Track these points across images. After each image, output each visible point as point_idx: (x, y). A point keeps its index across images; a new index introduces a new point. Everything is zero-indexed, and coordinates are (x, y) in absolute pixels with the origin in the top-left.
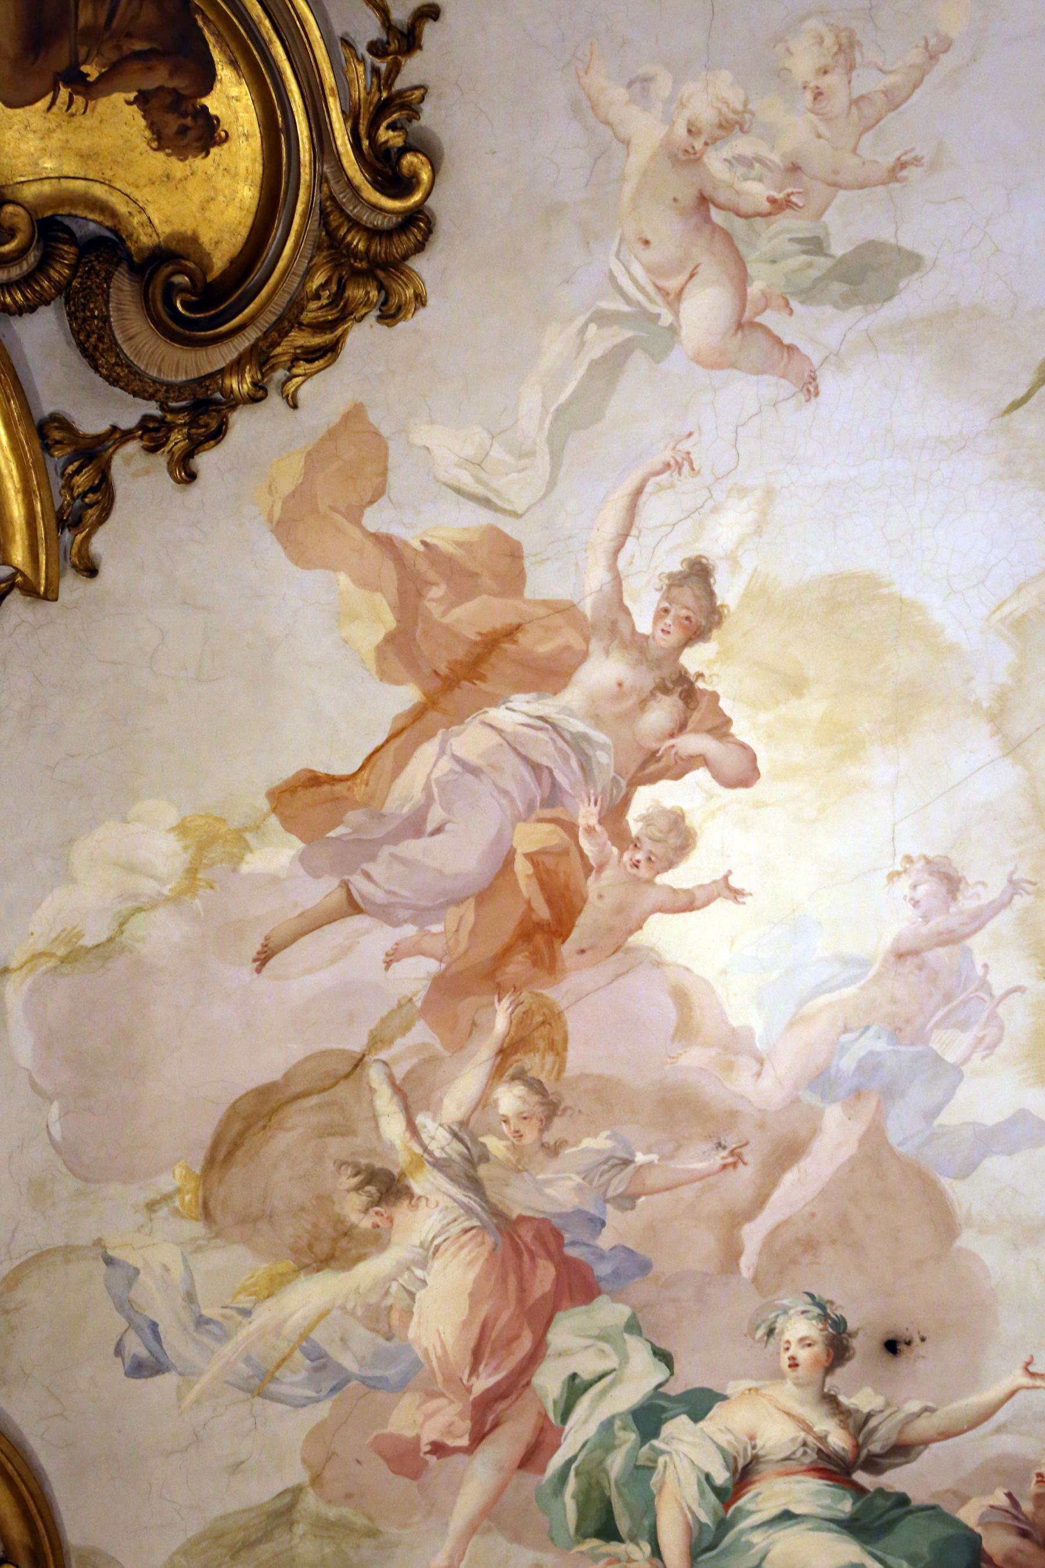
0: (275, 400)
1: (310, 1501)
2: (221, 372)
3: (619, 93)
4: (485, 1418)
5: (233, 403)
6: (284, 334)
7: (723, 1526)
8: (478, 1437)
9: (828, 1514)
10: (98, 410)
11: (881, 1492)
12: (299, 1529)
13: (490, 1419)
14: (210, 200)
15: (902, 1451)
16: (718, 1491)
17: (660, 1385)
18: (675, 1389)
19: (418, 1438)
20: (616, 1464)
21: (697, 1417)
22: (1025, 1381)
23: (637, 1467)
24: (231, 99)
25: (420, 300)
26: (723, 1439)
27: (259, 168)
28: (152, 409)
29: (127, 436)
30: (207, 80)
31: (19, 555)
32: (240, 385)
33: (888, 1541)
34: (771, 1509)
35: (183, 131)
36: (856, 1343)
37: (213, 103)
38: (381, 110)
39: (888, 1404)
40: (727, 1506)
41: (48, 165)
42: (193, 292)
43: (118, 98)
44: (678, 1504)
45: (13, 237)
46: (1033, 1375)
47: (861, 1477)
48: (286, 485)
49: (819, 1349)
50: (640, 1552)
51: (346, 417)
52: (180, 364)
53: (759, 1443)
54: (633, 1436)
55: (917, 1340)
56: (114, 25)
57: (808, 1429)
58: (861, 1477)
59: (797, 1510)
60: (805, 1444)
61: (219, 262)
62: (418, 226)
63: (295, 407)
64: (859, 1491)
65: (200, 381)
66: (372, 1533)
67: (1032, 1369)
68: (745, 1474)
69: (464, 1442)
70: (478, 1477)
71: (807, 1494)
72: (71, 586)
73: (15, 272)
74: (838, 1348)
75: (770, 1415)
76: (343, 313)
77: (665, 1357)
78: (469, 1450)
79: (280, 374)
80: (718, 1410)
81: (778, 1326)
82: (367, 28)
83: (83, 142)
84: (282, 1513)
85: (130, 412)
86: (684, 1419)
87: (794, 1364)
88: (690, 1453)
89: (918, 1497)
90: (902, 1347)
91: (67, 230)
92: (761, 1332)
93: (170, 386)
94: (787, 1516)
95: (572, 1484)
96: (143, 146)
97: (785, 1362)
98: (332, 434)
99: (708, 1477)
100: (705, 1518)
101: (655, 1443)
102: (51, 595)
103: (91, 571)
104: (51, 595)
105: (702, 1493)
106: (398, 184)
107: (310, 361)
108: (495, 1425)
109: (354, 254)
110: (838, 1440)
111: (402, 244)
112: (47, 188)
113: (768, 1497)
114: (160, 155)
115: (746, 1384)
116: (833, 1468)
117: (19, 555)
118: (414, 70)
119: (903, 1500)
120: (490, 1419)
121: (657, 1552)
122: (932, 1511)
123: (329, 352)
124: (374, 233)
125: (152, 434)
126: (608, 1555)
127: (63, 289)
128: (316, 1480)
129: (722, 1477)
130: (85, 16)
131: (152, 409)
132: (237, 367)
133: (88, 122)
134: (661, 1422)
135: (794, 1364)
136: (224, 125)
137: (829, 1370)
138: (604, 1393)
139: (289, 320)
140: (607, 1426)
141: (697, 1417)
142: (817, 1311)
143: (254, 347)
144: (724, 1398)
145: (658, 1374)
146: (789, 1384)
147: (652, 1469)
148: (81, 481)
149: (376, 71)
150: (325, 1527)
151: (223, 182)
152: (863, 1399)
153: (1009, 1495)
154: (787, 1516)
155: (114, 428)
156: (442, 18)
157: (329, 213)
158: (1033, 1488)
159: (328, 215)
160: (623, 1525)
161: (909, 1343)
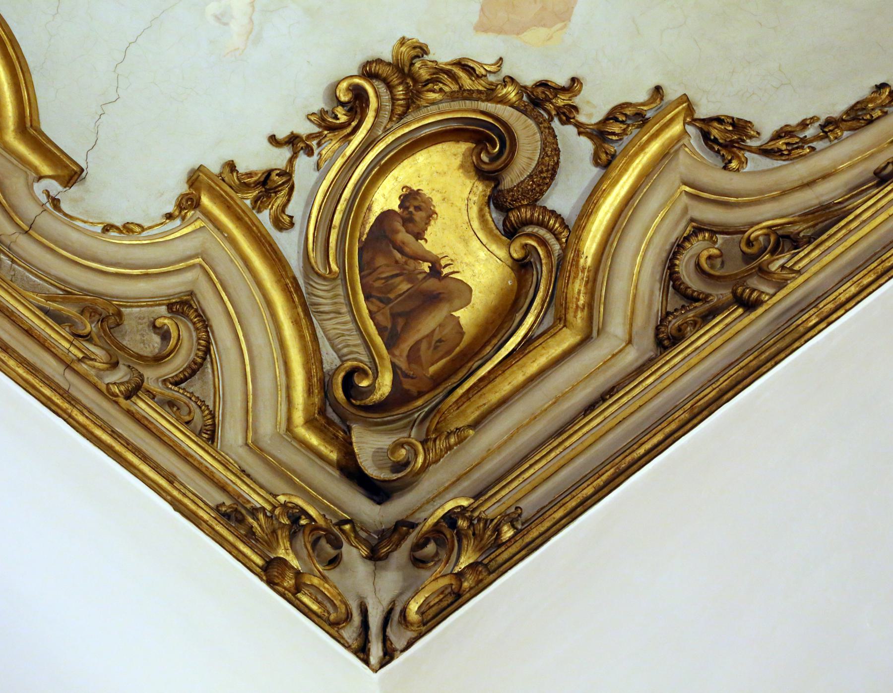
0: (506, 71)
2: (512, 106)
3: (234, 27)
5: (522, 89)
6: (471, 92)
10: (577, 148)
14: (440, 174)
24: (386, 197)
25: (403, 41)
27: (406, 162)
28: (556, 124)
29: (578, 125)
30: (386, 215)
31: (676, 128)
32: (511, 92)
35: (418, 208)
37: (395, 205)
38: (333, 128)
41: (482, 254)
42: (488, 147)
43: (428, 247)
45: (526, 245)
48: (543, 32)
51: (486, 31)
52: (525, 129)
56: (398, 272)
61: (463, 147)
62: (370, 71)
63: (501, 59)
65: (524, 112)
72: (672, 93)
73: (542, 232)
76: (439, 72)
79: (492, 78)
82: (304, 165)
83: (460, 247)
85: (566, 133)
91: (504, 224)
93: (538, 124)
96: (439, 220)
98: (500, 31)
102: (685, 98)
103: (658, 89)
104: (685, 98)
106: (359, 95)
107: (473, 69)
109: (407, 88)
111: (384, 71)
112: (494, 248)
114: (437, 210)
117: (676, 128)
118: (305, 128)
123: (461, 64)
124: (390, 87)
125: (567, 115)
127: (533, 204)
130: (405, 286)
131: (556, 124)
132: (503, 101)
133: (448, 251)
136: (400, 192)
139: (463, 94)
143: (489, 99)
148: (617, 128)
149: (319, 144)
151: (426, 174)
155: (580, 133)
156: (272, 134)
157: (399, 117)
159: (399, 115)
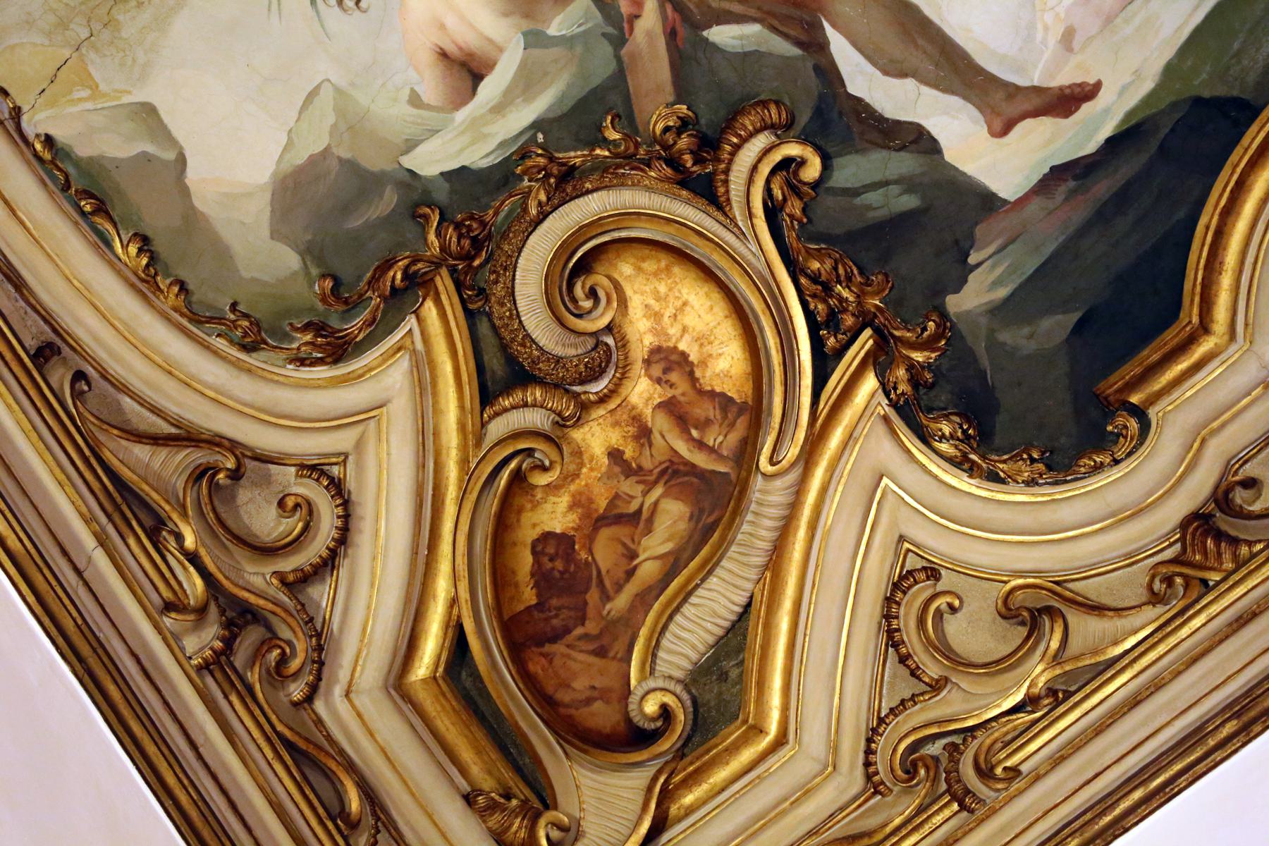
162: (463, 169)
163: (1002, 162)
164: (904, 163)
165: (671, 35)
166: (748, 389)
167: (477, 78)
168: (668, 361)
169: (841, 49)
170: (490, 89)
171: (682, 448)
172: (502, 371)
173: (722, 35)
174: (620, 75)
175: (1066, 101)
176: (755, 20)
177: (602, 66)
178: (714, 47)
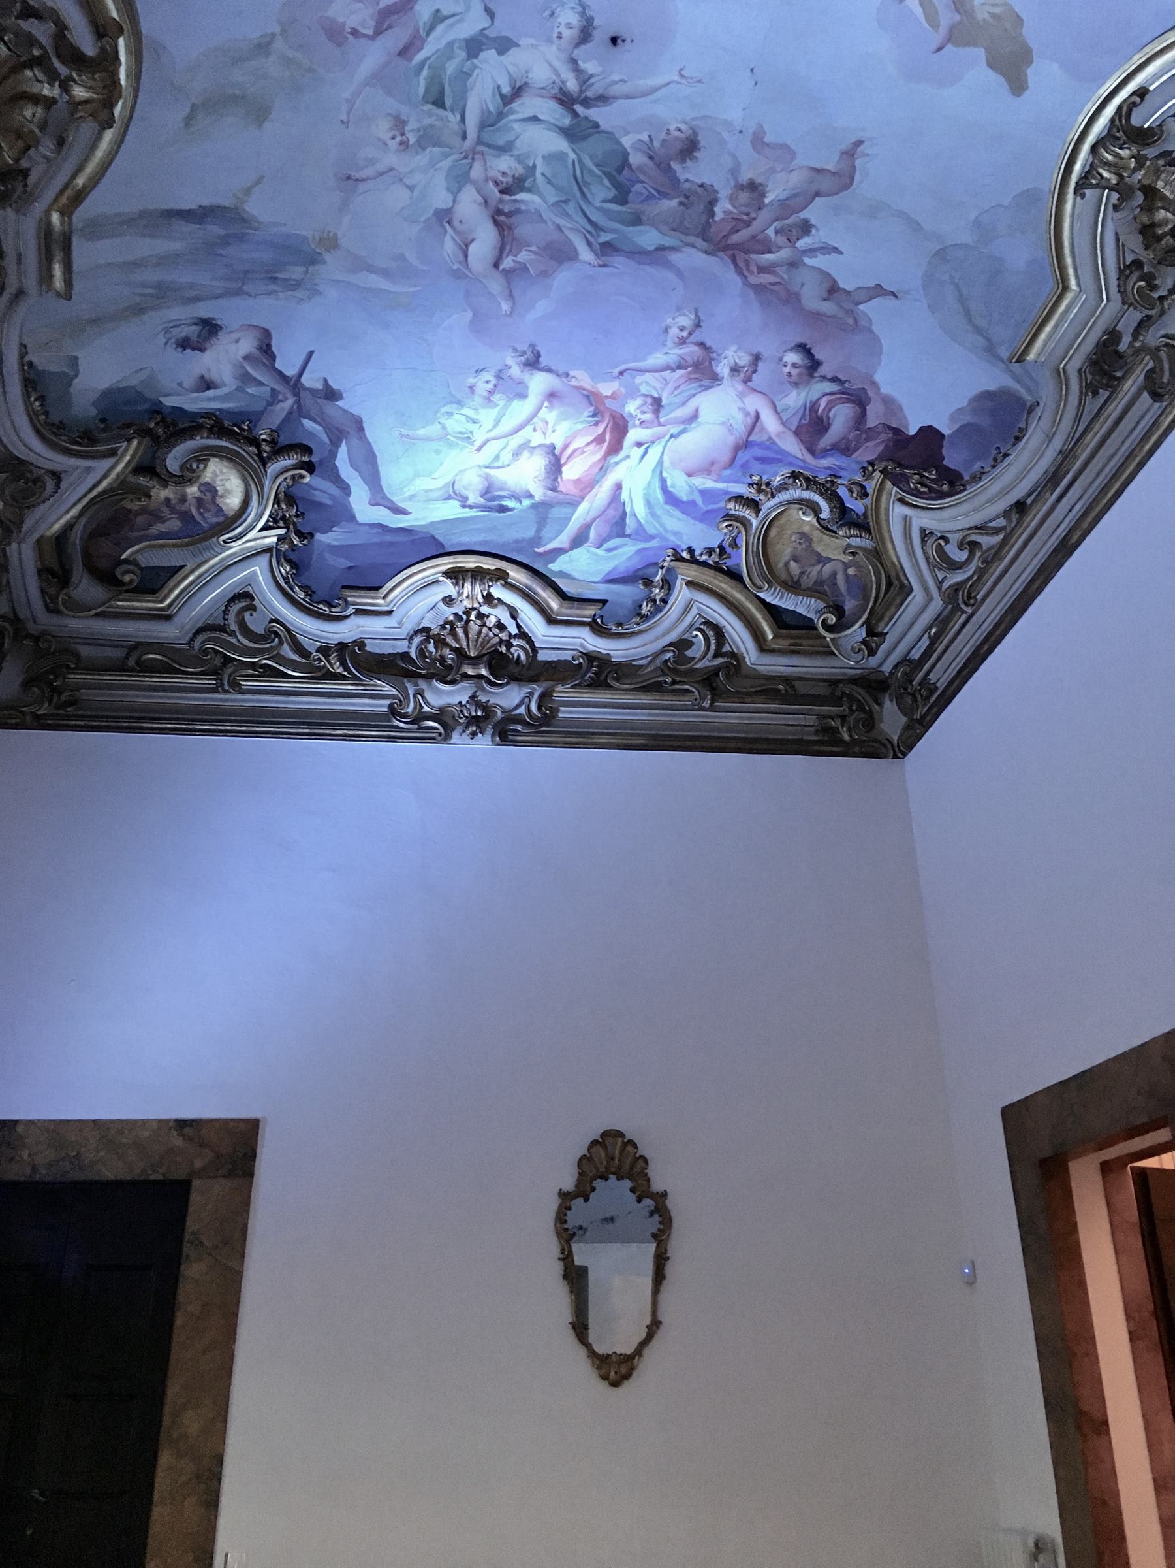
1: (279, 45)
4: (384, 21)
7: (501, 115)
8: (378, 32)
9: (558, 123)
11: (586, 118)
12: (271, 59)
13: (386, 24)
15: (603, 99)
16: (502, 96)
17: (484, 29)
18: (492, 33)
19: (344, 23)
20: (451, 67)
21: (502, 51)
22: (677, 78)
23: (462, 72)
26: (511, 69)
33: (585, 144)
34: (529, 113)
36: (596, 33)
39: (603, 72)
40: (505, 105)
44: (480, 97)
46: (682, 76)
47: (578, 108)
49: (575, 32)
50: (454, 118)
53: (530, 75)
54: (463, 55)
55: (628, 41)
57: (558, 75)
58: (578, 108)
59: (540, 117)
60: (554, 83)
64: (576, 115)
66: (311, 70)
67: (683, 73)
68: (518, 91)
69: (370, 32)
70: (373, 56)
71: (550, 110)
74: (585, 34)
75: (541, 62)
77: (491, 14)
78: (372, 38)
80: (513, 51)
81: (557, 12)
84: (263, 47)
86: (493, 51)
87: (560, 37)
88: (491, 74)
89: (604, 125)
90: (619, 41)
92: (547, 13)
94: (535, 119)
95: (425, 72)
97: (555, 35)
99: (499, 87)
100: (492, 109)
101: (475, 61)
105: (493, 95)
108: (390, 27)
110: (572, 85)
113: (527, 106)
115: (531, 41)
116: (565, 100)
119: (596, 125)
120: (386, 24)
121: (463, 119)
122: (610, 135)
126: (437, 115)
128: (284, 32)
129: (506, 90)
134: (481, 50)
135: (560, 37)
137: (577, 45)
138: (452, 25)
140: (450, 45)
141: (502, 51)
142: (580, 9)
144: (517, 45)
145: (485, 22)
146: (554, 48)
147: (469, 75)
150: (288, 62)
152: (590, 67)
153: (650, 136)
154: (535, 119)
158: (663, 135)
160: (448, 102)
161: (623, 41)
162: (181, 409)
163: (363, 508)
164: (334, 490)
165: (290, 413)
166: (231, 513)
167: (209, 388)
168: (210, 489)
169: (343, 451)
170: (210, 393)
171: (194, 511)
172: (147, 468)
173: (307, 423)
174: (262, 413)
175: (398, 510)
176: (320, 425)
177: (258, 407)
178: (302, 425)
